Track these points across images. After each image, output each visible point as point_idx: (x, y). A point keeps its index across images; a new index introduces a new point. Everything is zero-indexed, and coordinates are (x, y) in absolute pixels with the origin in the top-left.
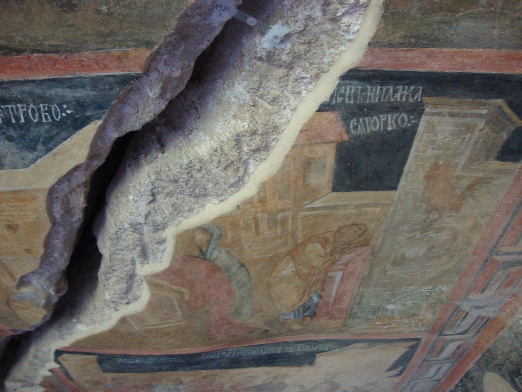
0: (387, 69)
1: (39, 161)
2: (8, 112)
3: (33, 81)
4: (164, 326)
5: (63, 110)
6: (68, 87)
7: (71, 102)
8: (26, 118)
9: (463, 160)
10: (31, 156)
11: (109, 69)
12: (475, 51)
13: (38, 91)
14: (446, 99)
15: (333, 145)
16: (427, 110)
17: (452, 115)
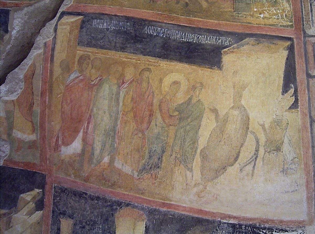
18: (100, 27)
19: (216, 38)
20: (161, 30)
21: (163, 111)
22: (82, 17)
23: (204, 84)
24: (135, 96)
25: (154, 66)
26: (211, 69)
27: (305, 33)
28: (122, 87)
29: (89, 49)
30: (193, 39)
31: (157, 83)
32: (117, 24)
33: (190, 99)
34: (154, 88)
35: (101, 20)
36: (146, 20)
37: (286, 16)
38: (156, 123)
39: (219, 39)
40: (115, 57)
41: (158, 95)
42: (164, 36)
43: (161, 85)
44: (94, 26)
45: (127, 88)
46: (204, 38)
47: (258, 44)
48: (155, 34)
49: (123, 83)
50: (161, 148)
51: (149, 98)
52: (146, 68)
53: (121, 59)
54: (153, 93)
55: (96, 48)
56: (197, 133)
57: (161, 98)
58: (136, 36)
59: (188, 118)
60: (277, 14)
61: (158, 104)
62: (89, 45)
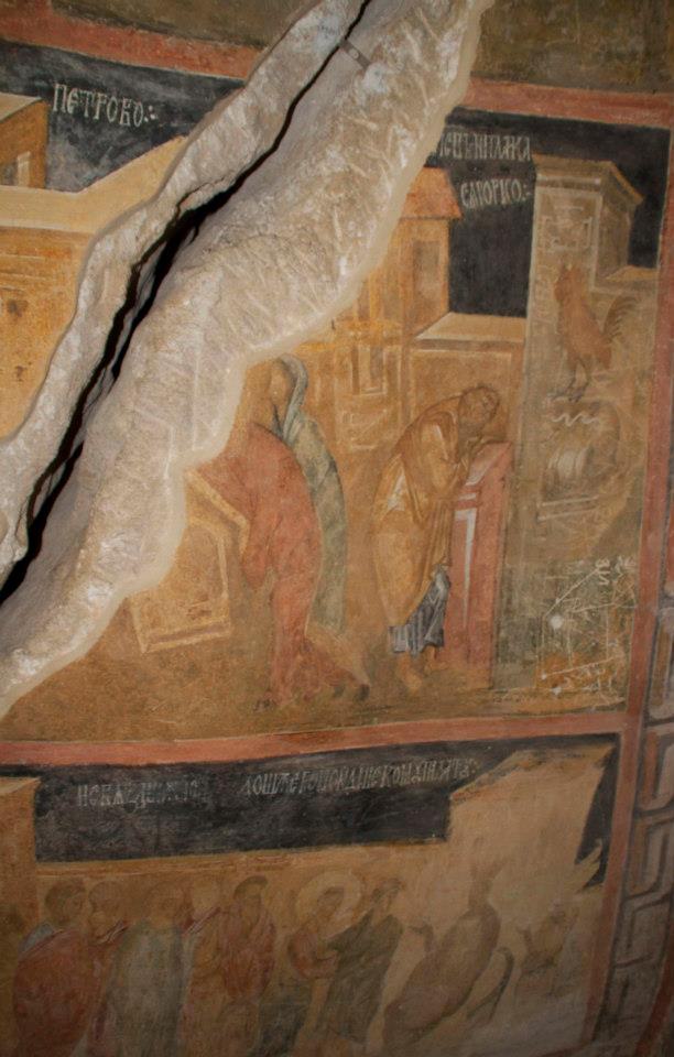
0: (491, 111)
1: (96, 185)
2: (84, 101)
3: (126, 67)
4: (194, 640)
5: (147, 114)
6: (161, 83)
7: (158, 103)
8: (102, 114)
9: (592, 265)
10: (89, 174)
11: (211, 69)
12: (570, 91)
13: (128, 80)
14: (555, 159)
15: (445, 223)
16: (540, 176)
17: (567, 185)
18: (102, 804)
19: (438, 765)
20: (291, 776)
22: (34, 779)
24: (226, 941)
25: (274, 868)
26: (422, 843)
27: (646, 714)
29: (74, 867)
30: (378, 779)
32: (157, 790)
33: (367, 918)
35: (103, 786)
36: (247, 763)
37: (614, 682)
39: (446, 766)
42: (300, 792)
44: (83, 803)
46: (407, 770)
47: (540, 763)
48: (274, 792)
49: (190, 922)
55: (99, 859)
58: (219, 809)
59: (360, 956)
60: (593, 681)
62: (73, 854)
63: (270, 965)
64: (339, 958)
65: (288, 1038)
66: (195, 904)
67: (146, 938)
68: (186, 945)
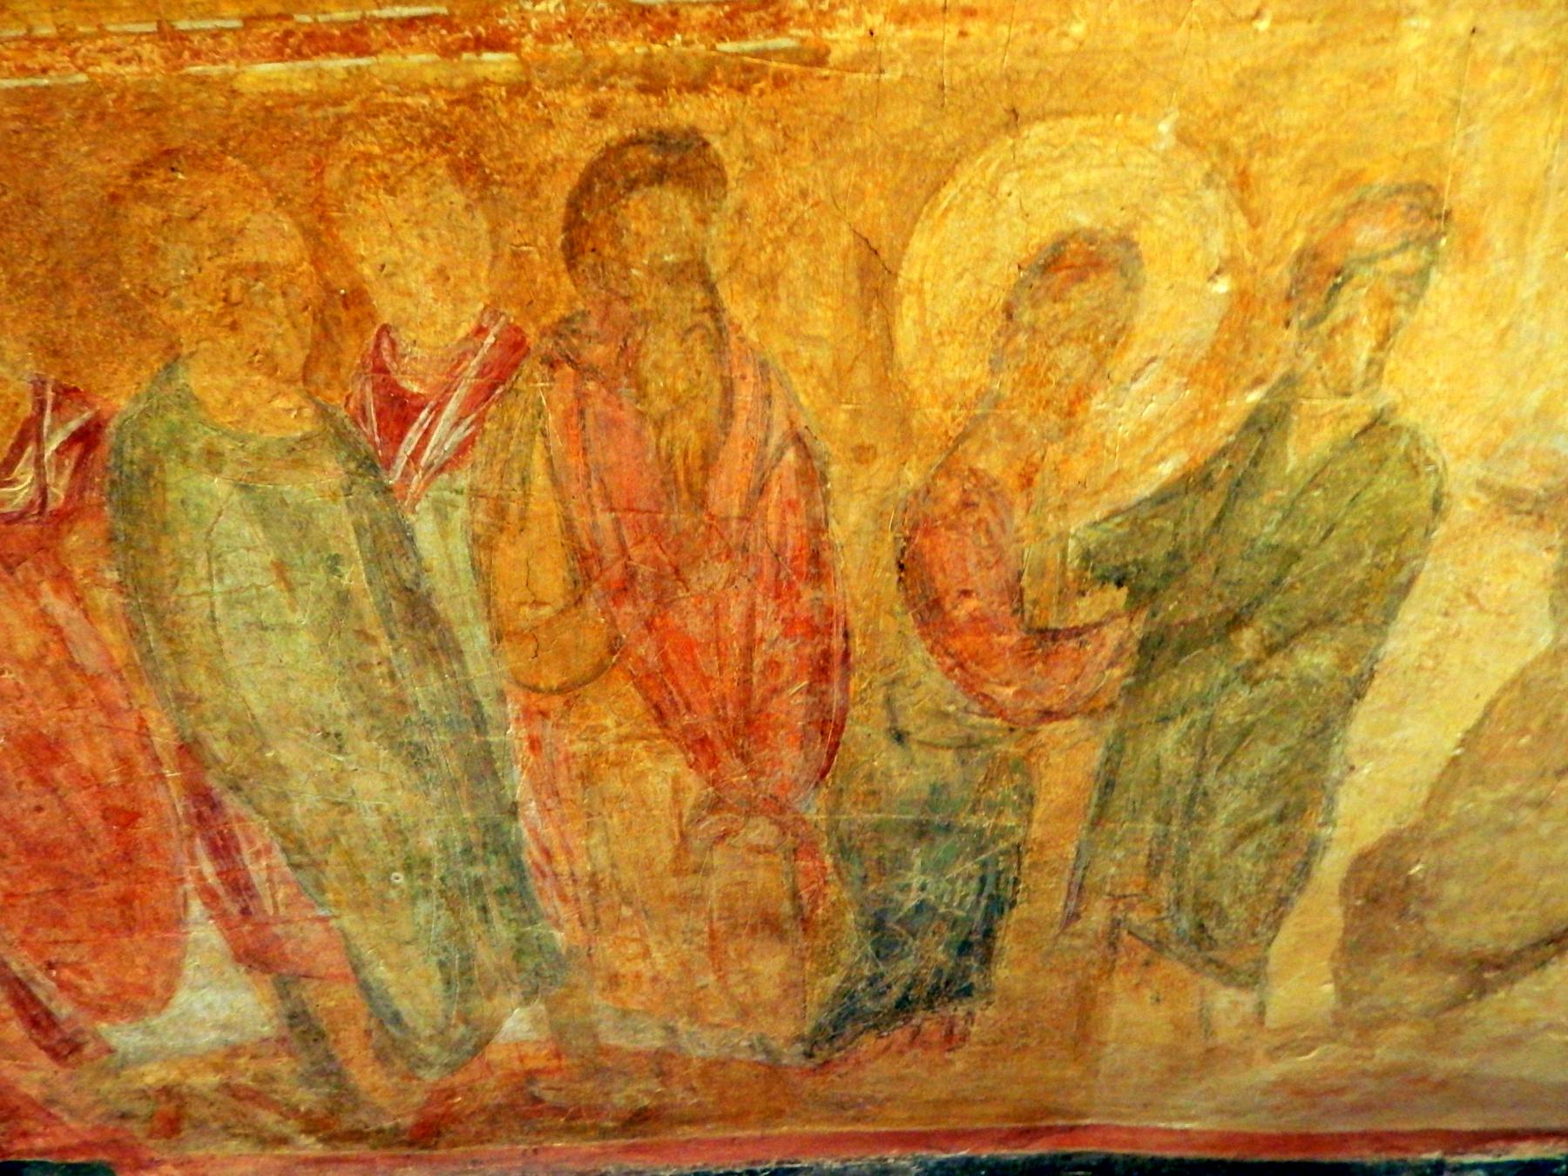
21: (963, 611)
23: (1462, 196)
25: (744, 78)
28: (400, 463)
31: (822, 317)
34: (807, 394)
38: (894, 720)
40: (107, 67)
41: (863, 454)
43: (888, 329)
45: (478, 453)
50: (974, 884)
51: (772, 515)
52: (636, 142)
53: (202, 81)
54: (806, 453)
56: (1324, 732)
57: (913, 477)
59: (1236, 622)
61: (887, 556)
63: (837, 643)
64: (1138, 628)
65: (965, 948)
66: (387, 306)
67: (219, 486)
68: (425, 529)
